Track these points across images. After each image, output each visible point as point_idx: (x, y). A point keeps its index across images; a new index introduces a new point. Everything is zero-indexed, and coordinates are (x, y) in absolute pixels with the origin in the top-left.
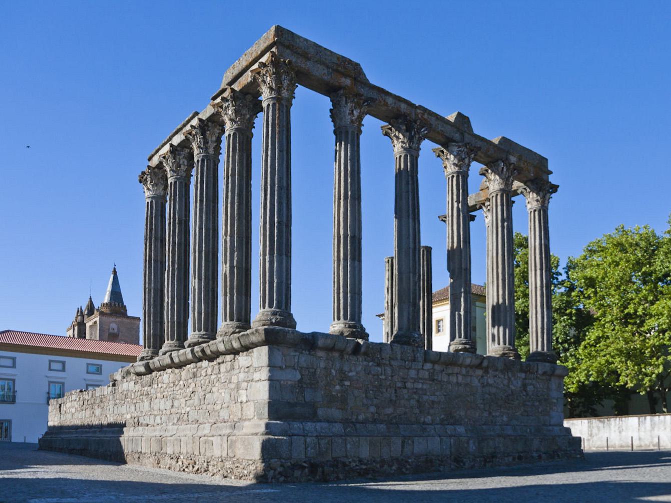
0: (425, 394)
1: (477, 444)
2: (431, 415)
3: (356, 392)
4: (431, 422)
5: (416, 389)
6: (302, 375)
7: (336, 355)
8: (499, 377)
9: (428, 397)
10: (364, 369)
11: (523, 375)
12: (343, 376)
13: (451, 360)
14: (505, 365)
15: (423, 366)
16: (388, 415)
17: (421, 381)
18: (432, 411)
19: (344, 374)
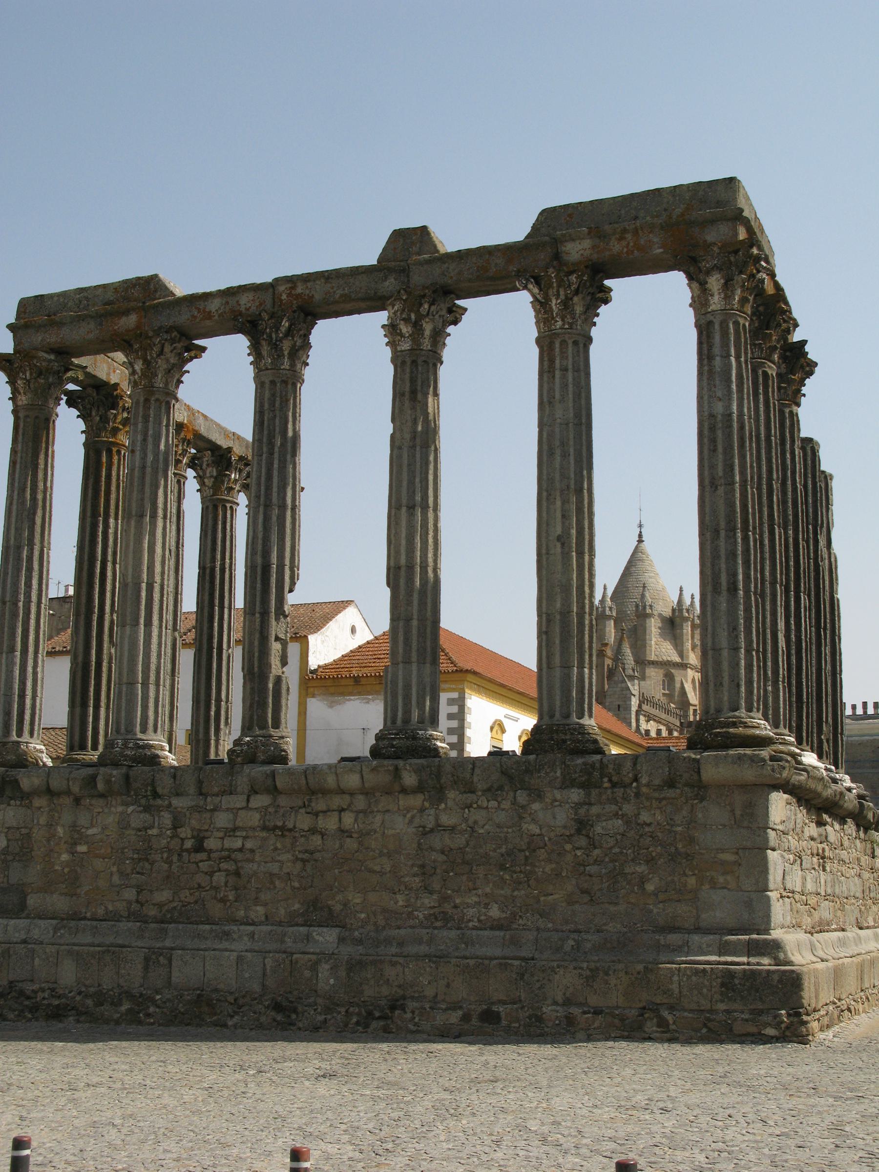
0: (252, 861)
1: (343, 973)
2: (265, 905)
3: (99, 864)
4: (263, 919)
5: (229, 850)
6: (8, 840)
7: (67, 801)
8: (479, 807)
9: (255, 867)
10: (117, 820)
11: (575, 795)
12: (76, 836)
13: (304, 782)
14: (502, 772)
15: (248, 801)
16: (160, 905)
17: (238, 834)
18: (264, 896)
19: (79, 832)
